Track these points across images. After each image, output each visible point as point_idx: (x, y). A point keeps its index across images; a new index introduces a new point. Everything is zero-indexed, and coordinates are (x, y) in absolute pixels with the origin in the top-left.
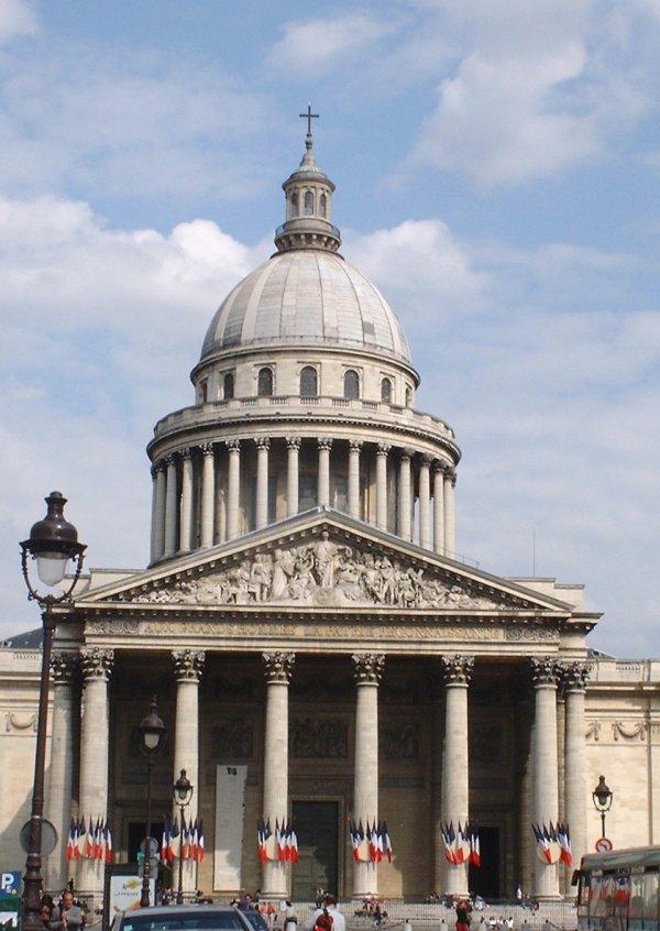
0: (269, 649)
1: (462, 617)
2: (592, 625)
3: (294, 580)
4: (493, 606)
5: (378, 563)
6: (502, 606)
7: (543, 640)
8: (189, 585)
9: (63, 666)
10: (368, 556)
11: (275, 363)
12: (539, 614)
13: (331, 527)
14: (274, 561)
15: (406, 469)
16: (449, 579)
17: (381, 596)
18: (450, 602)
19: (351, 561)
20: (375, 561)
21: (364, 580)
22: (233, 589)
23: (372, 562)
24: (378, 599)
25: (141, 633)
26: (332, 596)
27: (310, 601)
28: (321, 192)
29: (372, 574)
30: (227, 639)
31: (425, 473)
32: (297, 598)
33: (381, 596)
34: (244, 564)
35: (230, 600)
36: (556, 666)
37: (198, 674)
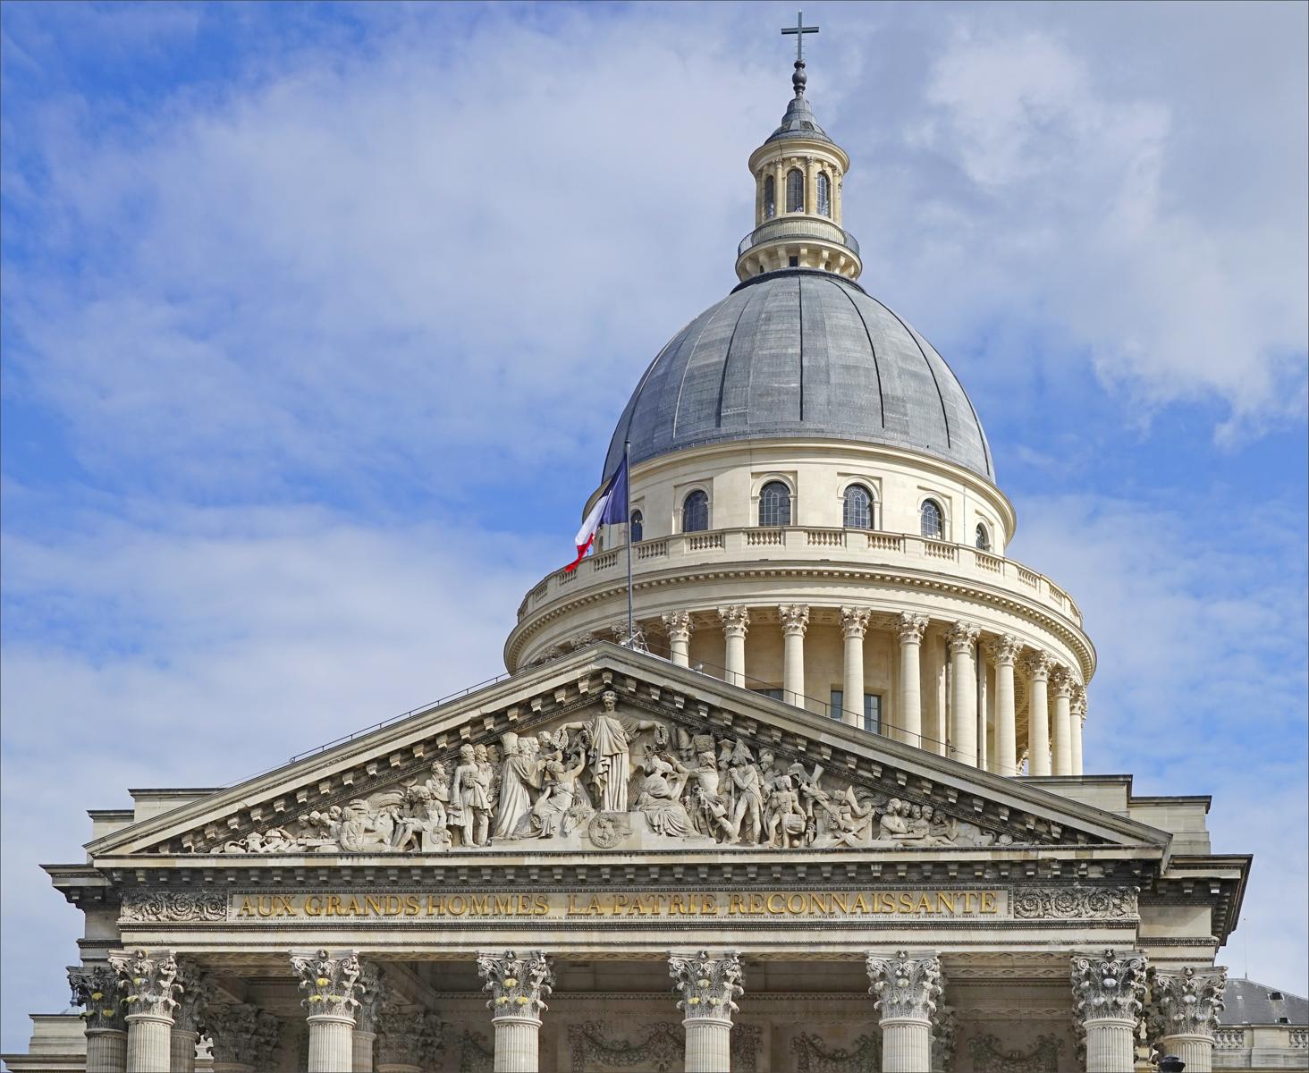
0: (487, 949)
1: (910, 865)
3: (543, 799)
4: (986, 840)
5: (726, 755)
6: (1005, 840)
7: (1098, 916)
8: (325, 816)
9: (97, 996)
10: (703, 740)
12: (1086, 855)
16: (886, 784)
17: (733, 827)
18: (883, 832)
20: (718, 750)
21: (694, 794)
22: (414, 824)
23: (711, 755)
24: (722, 834)
26: (622, 830)
27: (575, 841)
29: (712, 780)
32: (548, 836)
33: (733, 827)
34: (439, 766)
35: (410, 842)
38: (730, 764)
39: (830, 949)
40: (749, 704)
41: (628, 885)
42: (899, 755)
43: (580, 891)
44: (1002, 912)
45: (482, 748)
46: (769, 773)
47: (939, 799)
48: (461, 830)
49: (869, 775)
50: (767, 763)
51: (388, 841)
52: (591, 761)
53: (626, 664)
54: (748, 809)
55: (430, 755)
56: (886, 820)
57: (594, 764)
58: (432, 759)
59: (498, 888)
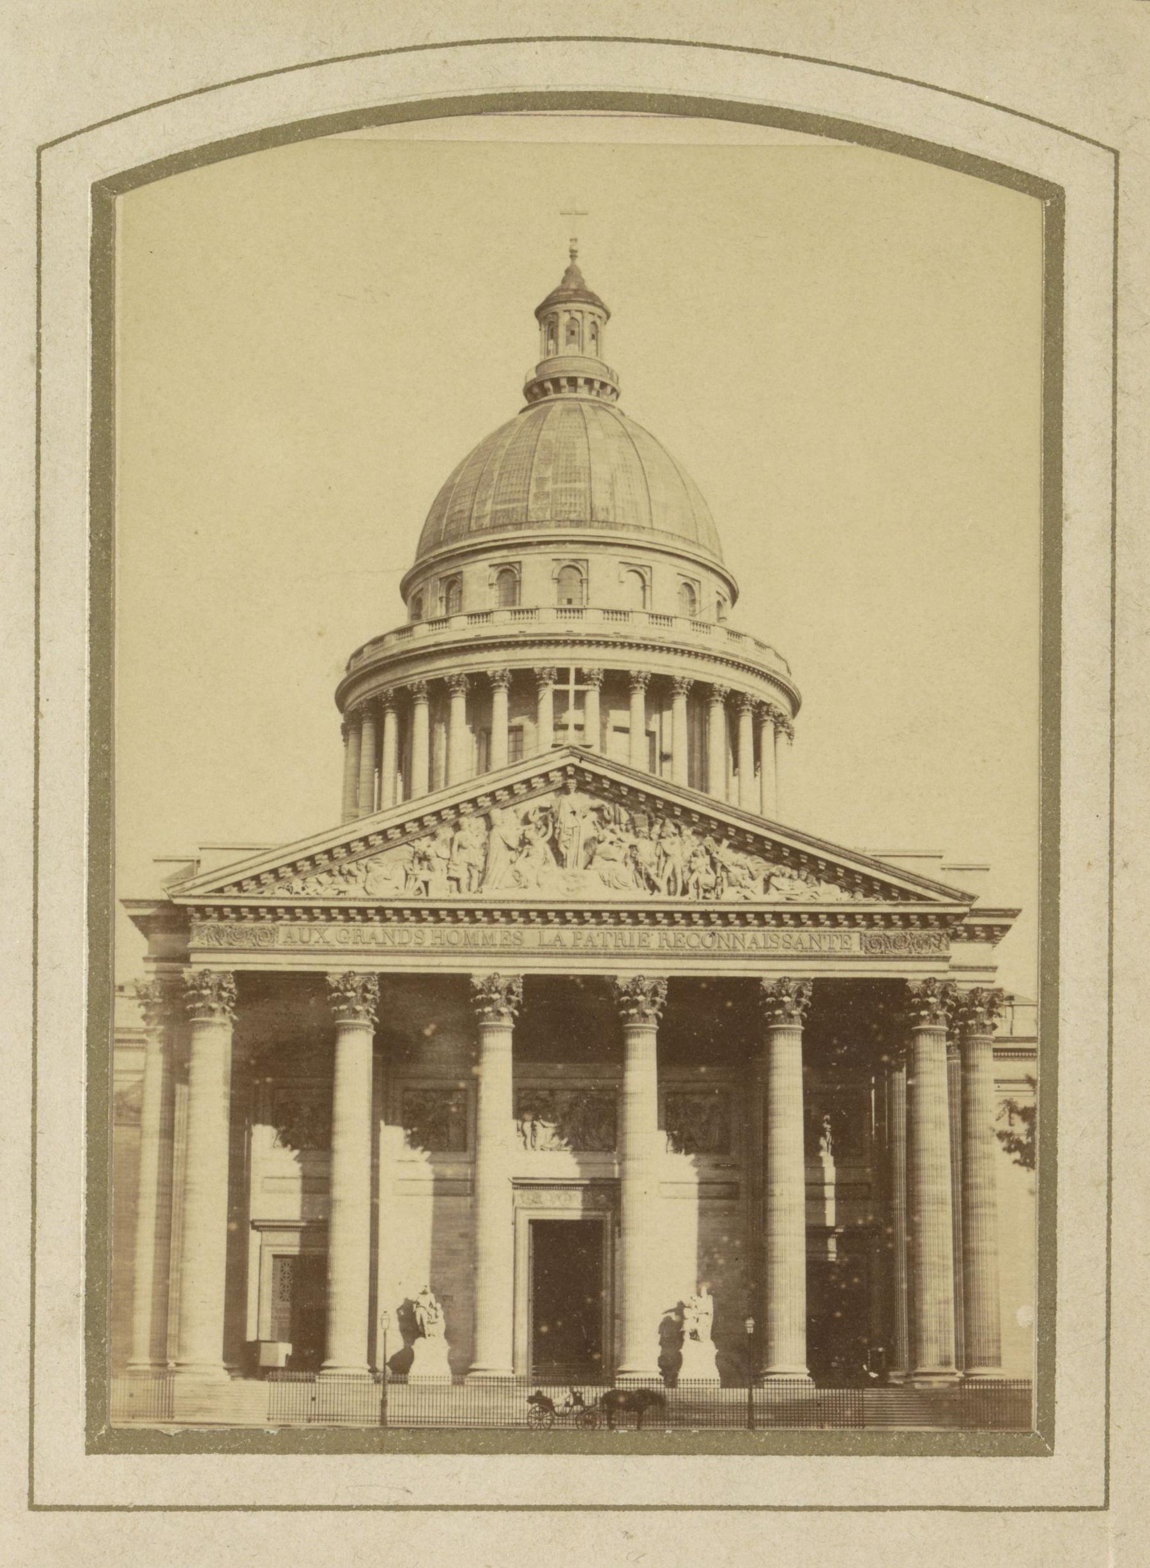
2: (1005, 928)
4: (845, 897)
6: (859, 896)
11: (520, 562)
13: (580, 771)
14: (490, 827)
15: (718, 714)
18: (772, 890)
19: (612, 826)
20: (651, 825)
23: (645, 829)
24: (653, 887)
25: (277, 946)
28: (590, 318)
29: (647, 850)
30: (413, 953)
31: (746, 724)
33: (662, 883)
35: (419, 889)
36: (945, 994)
38: (660, 837)
44: (856, 950)
45: (473, 820)
48: (457, 880)
51: (402, 887)
52: (557, 831)
54: (674, 870)
56: (774, 880)
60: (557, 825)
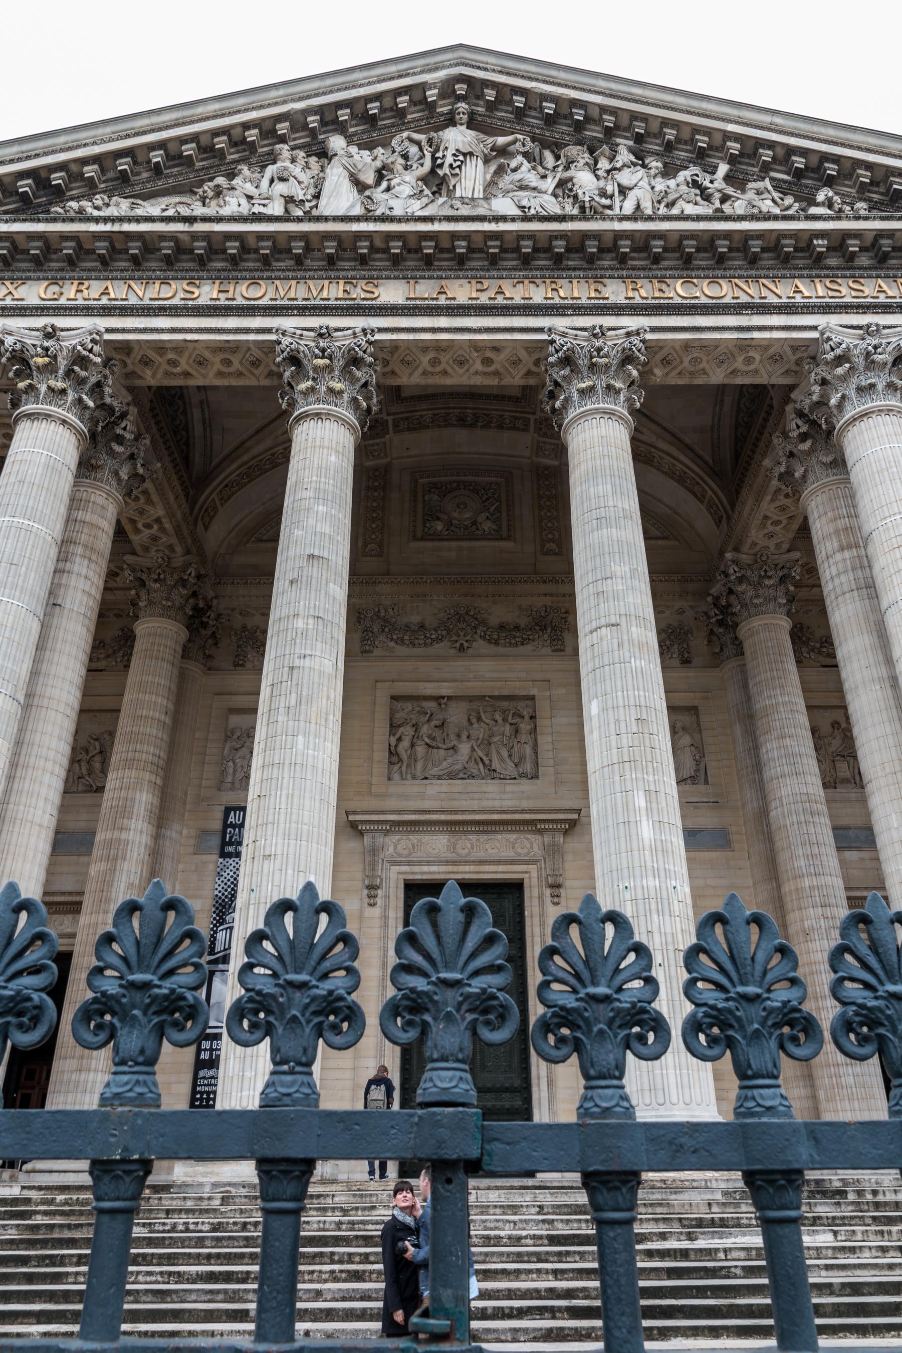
5: (604, 164)
10: (573, 150)
13: (475, 86)
37: (80, 400)
39: (766, 335)
40: (637, 98)
41: (488, 270)
42: (830, 139)
43: (424, 278)
45: (301, 154)
46: (659, 179)
47: (876, 197)
49: (785, 177)
50: (657, 168)
53: (486, 69)
55: (236, 156)
57: (441, 166)
58: (238, 162)
59: (312, 273)
60: (439, 154)
